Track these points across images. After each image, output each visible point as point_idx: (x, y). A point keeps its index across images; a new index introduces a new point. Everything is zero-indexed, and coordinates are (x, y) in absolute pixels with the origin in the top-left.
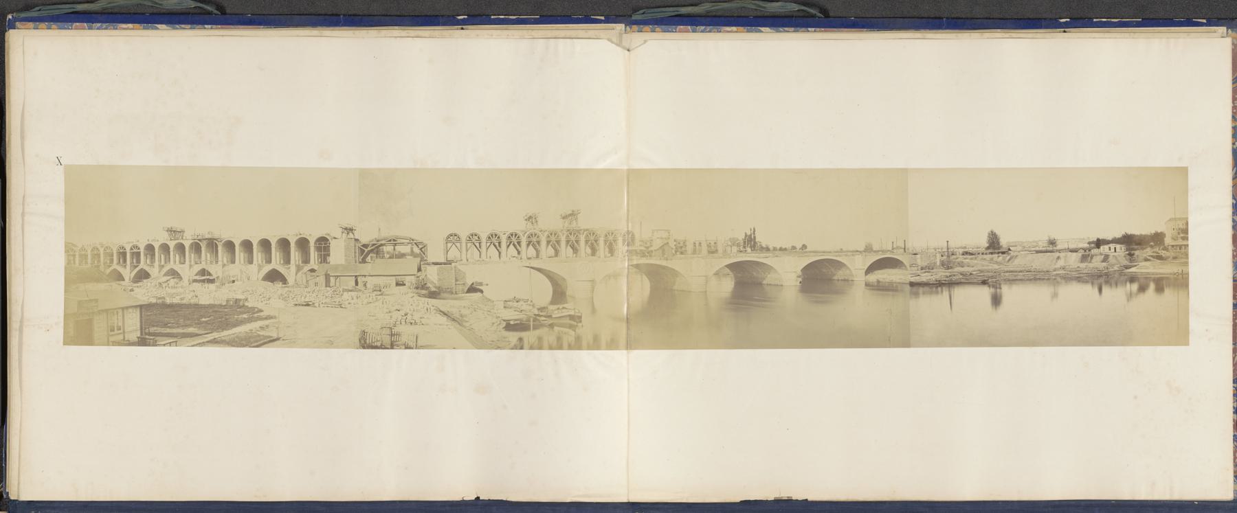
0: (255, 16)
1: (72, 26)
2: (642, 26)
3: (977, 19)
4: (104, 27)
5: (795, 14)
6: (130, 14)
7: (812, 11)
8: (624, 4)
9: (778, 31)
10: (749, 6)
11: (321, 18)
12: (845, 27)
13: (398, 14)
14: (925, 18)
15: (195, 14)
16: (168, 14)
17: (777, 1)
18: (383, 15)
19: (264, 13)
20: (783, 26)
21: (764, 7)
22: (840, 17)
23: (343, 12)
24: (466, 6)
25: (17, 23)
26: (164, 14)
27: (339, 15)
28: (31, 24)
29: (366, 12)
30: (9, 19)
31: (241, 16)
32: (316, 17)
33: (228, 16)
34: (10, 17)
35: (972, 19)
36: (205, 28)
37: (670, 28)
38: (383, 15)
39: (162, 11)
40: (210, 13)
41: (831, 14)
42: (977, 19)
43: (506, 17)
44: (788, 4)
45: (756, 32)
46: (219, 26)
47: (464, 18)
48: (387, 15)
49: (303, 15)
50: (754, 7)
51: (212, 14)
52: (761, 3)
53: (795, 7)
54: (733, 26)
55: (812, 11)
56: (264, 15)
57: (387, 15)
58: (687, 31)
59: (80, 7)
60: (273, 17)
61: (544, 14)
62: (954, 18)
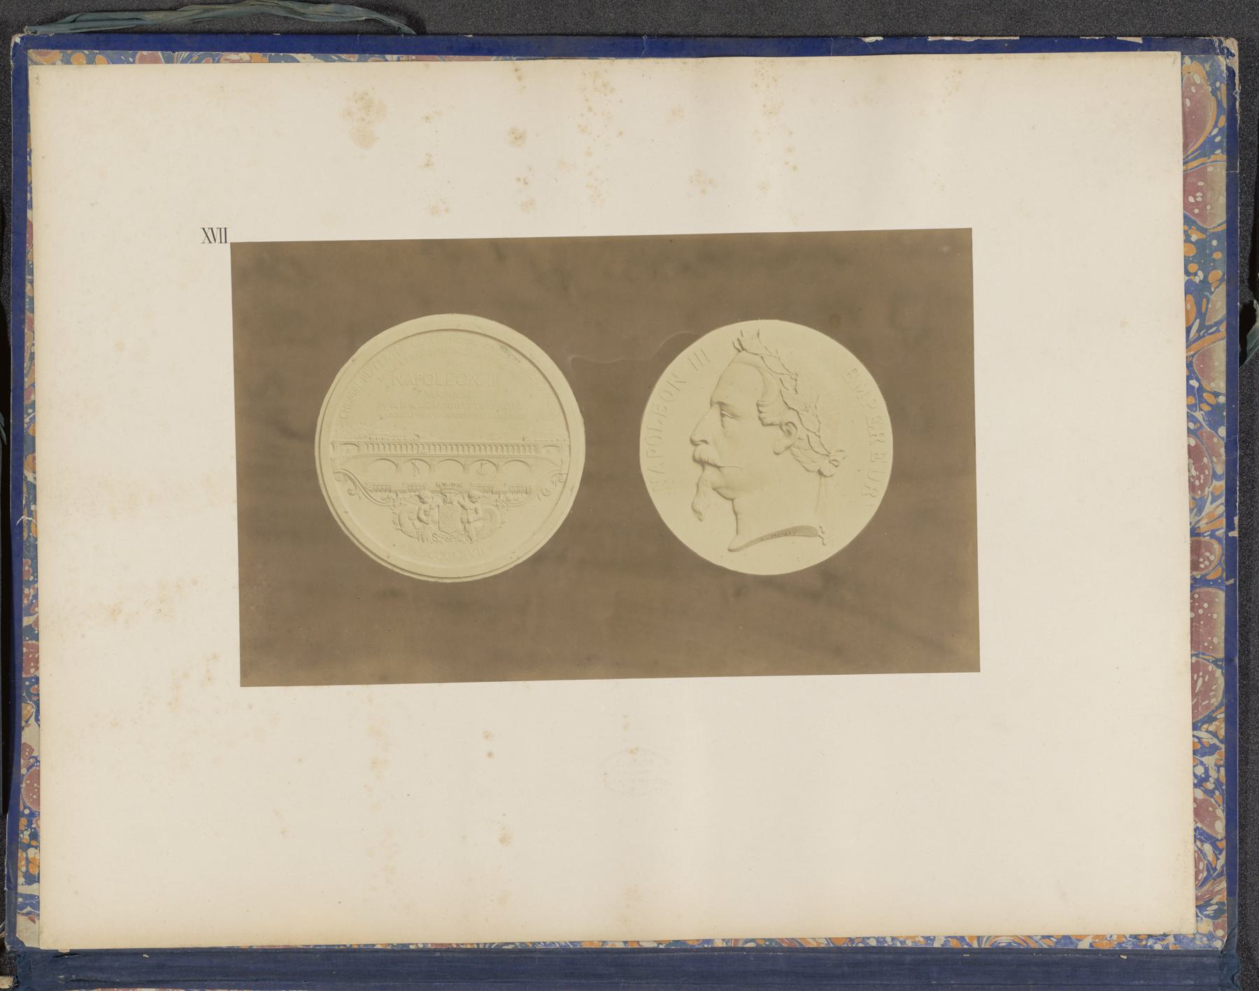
0: (481, 38)
1: (134, 57)
2: (70, 51)
3: (706, 36)
4: (195, 58)
5: (361, 28)
6: (244, 33)
7: (394, 22)
8: (1180, 14)
9: (327, 61)
10: (274, 11)
11: (604, 40)
12: (455, 53)
13: (753, 32)
14: (608, 35)
15: (368, 33)
16: (317, 33)
17: (328, 3)
18: (722, 36)
19: (498, 31)
20: (338, 50)
21: (302, 14)
22: (446, 34)
23: (647, 30)
24: (880, 17)
25: (30, 51)
26: (309, 33)
27: (640, 36)
28: (57, 54)
29: (690, 30)
30: (16, 44)
31: (454, 38)
32: (596, 38)
33: (429, 36)
34: (17, 39)
35: (696, 36)
36: (386, 61)
37: (123, 54)
38: (722, 36)
39: (306, 28)
40: (395, 32)
41: (430, 27)
42: (706, 36)
43: (957, 38)
44: (347, 8)
45: (286, 61)
46: (414, 57)
47: (877, 41)
48: (730, 36)
49: (572, 35)
50: (282, 13)
51: (400, 34)
52: (296, 6)
53: (361, 14)
54: (242, 51)
55: (394, 22)
56: (498, 35)
57: (730, 36)
58: (156, 61)
59: (151, 19)
60: (514, 38)
61: (1029, 32)
62: (662, 36)
